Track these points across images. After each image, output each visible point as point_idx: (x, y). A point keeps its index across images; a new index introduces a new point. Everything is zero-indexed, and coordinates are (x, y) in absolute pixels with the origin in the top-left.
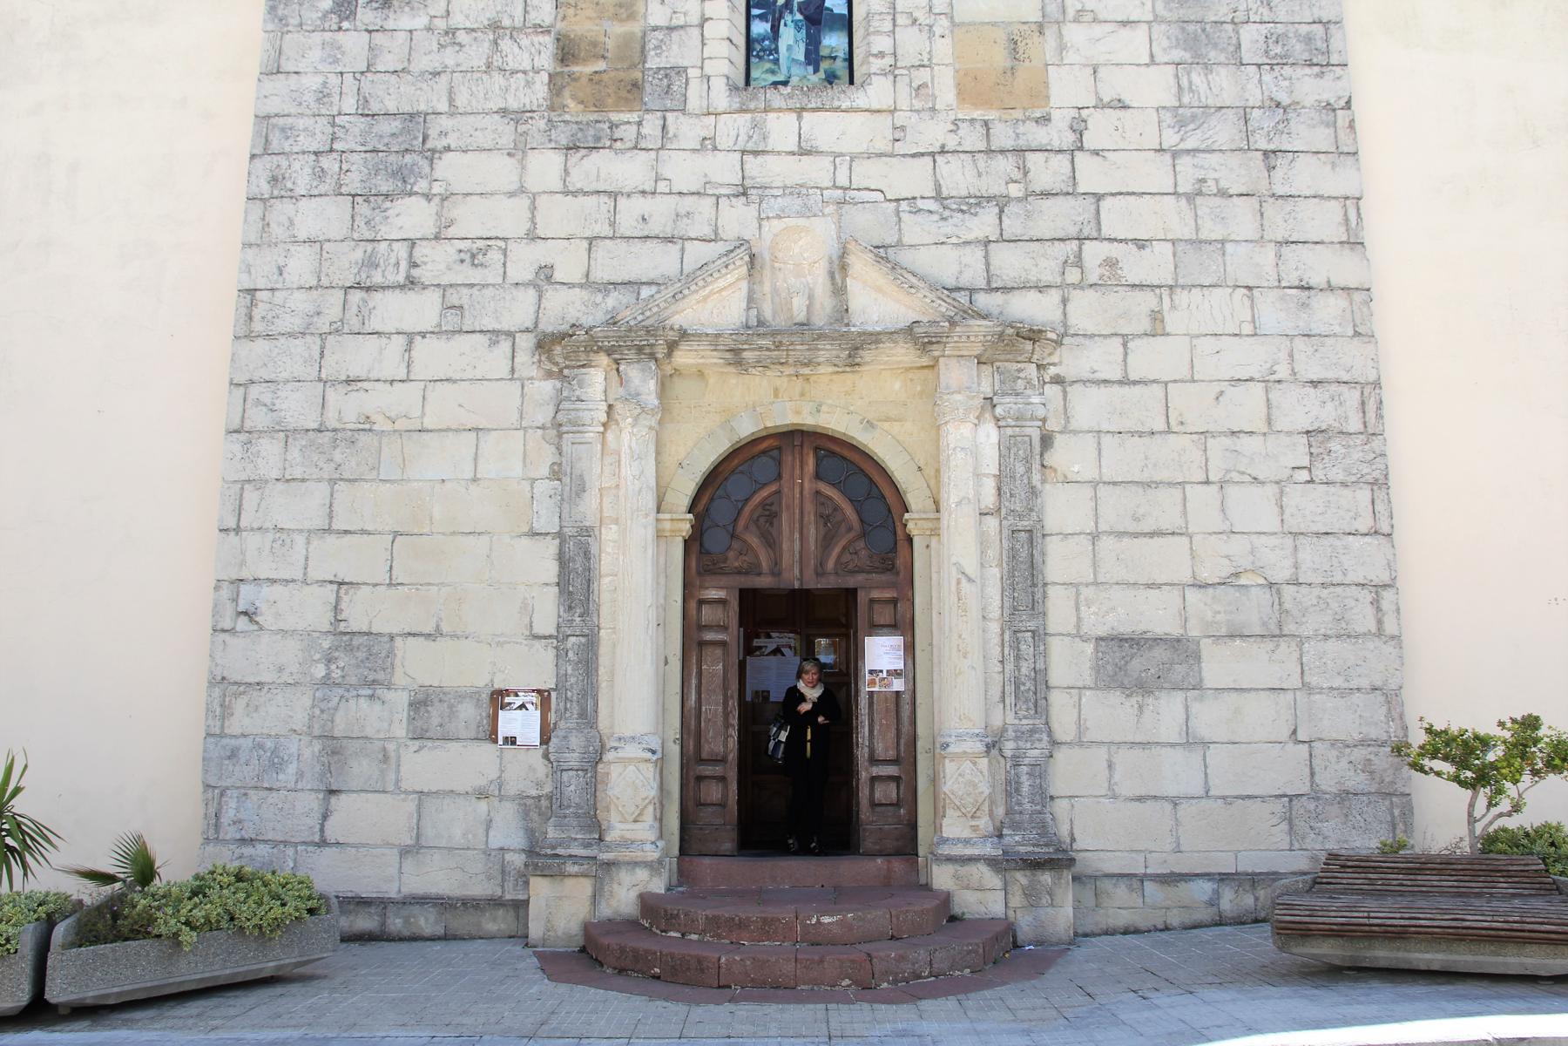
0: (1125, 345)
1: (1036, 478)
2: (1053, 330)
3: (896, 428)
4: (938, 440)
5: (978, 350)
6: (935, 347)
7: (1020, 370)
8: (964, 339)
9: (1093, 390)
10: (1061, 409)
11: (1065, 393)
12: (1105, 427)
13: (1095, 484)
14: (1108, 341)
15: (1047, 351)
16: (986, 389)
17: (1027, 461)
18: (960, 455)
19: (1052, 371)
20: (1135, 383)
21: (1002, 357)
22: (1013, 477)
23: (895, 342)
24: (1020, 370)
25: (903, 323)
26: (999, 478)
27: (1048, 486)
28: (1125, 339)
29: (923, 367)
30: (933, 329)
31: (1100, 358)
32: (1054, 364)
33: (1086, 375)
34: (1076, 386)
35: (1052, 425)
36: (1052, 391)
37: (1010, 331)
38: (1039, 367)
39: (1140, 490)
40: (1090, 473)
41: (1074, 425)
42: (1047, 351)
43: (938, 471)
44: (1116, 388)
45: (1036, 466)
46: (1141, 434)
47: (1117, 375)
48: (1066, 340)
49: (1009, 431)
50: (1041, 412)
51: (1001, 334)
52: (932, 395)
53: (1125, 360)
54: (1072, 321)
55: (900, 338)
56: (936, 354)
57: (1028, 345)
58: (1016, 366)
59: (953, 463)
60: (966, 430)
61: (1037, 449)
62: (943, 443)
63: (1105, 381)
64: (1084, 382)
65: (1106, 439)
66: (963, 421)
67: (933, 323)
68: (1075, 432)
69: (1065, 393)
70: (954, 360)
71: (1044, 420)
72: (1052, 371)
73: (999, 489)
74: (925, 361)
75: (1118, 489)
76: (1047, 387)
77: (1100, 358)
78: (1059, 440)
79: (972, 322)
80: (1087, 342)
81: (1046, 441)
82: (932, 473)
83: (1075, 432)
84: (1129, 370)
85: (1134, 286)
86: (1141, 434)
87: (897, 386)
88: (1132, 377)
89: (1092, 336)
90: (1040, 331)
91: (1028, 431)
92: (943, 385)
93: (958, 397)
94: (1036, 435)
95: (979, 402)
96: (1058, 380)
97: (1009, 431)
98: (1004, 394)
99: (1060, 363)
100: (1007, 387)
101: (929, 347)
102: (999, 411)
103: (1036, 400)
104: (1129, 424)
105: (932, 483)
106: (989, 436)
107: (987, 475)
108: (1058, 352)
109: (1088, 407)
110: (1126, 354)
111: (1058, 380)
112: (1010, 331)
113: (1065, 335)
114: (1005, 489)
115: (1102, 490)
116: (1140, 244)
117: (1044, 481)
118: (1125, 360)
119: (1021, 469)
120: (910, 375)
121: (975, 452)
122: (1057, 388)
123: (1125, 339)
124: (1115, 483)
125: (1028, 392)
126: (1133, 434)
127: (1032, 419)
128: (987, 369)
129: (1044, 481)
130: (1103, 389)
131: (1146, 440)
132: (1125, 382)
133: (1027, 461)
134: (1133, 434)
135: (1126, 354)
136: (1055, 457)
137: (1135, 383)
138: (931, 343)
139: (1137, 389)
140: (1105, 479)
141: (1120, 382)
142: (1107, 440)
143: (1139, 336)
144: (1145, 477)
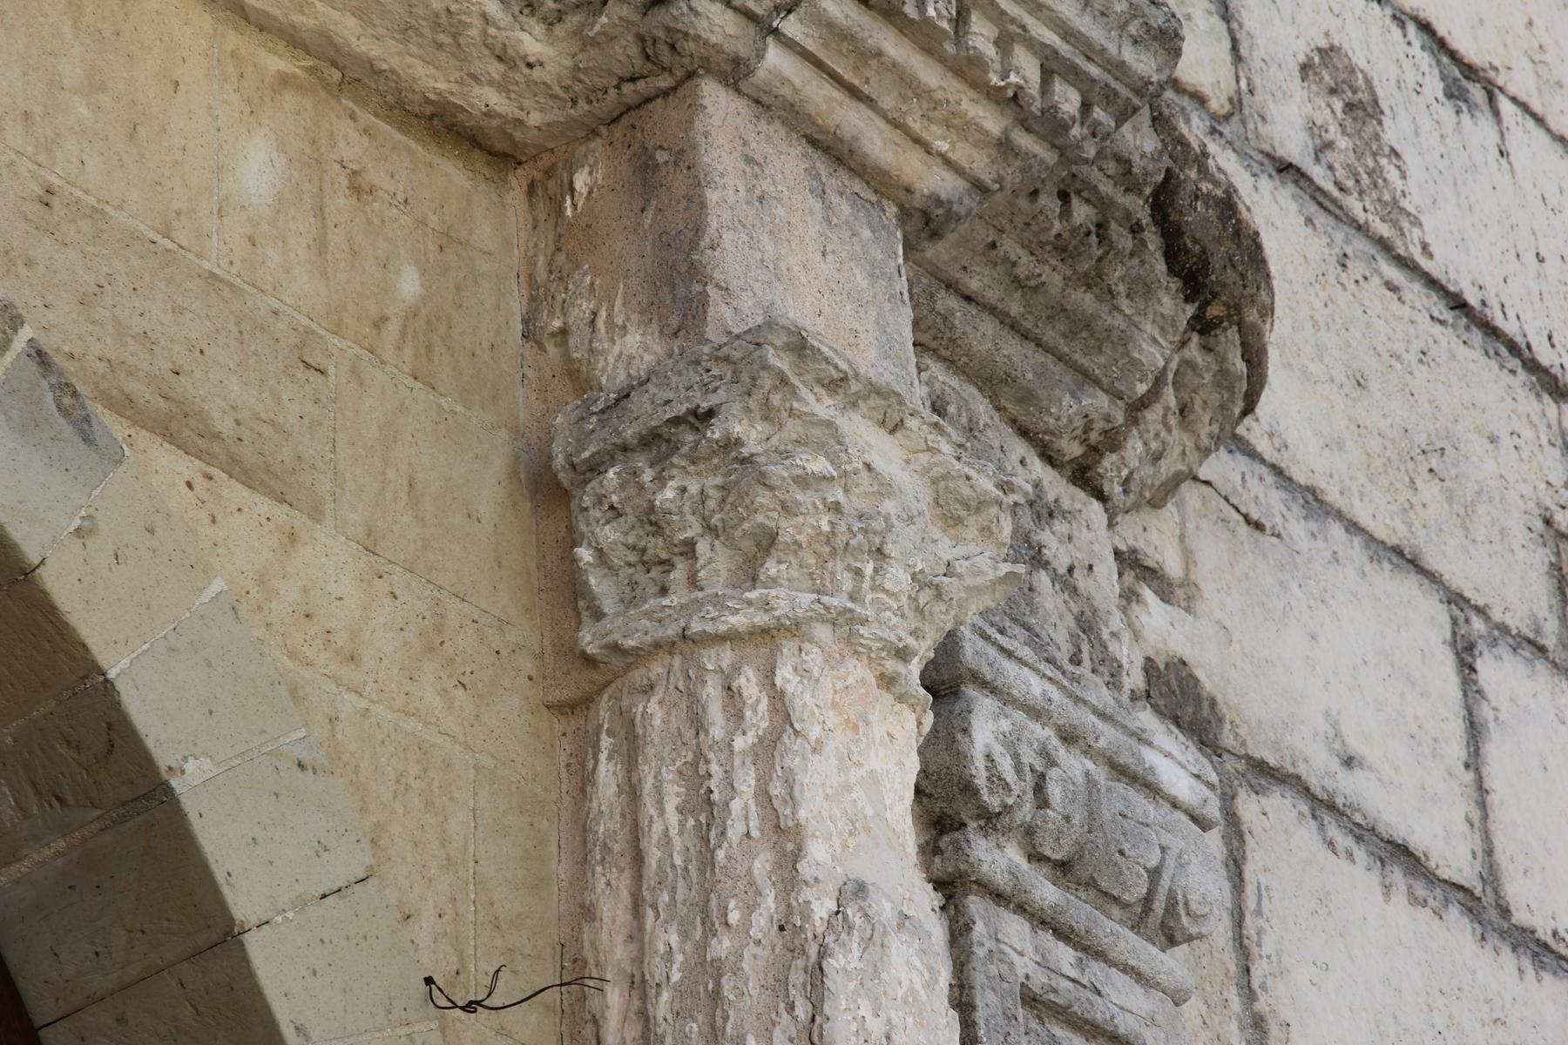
19: (1160, 627)
29: (447, 128)
57: (1155, 332)
72: (1160, 627)
80: (1298, 529)
85: (1458, 304)
87: (258, 170)
89: (1313, 502)
116: (1467, 81)
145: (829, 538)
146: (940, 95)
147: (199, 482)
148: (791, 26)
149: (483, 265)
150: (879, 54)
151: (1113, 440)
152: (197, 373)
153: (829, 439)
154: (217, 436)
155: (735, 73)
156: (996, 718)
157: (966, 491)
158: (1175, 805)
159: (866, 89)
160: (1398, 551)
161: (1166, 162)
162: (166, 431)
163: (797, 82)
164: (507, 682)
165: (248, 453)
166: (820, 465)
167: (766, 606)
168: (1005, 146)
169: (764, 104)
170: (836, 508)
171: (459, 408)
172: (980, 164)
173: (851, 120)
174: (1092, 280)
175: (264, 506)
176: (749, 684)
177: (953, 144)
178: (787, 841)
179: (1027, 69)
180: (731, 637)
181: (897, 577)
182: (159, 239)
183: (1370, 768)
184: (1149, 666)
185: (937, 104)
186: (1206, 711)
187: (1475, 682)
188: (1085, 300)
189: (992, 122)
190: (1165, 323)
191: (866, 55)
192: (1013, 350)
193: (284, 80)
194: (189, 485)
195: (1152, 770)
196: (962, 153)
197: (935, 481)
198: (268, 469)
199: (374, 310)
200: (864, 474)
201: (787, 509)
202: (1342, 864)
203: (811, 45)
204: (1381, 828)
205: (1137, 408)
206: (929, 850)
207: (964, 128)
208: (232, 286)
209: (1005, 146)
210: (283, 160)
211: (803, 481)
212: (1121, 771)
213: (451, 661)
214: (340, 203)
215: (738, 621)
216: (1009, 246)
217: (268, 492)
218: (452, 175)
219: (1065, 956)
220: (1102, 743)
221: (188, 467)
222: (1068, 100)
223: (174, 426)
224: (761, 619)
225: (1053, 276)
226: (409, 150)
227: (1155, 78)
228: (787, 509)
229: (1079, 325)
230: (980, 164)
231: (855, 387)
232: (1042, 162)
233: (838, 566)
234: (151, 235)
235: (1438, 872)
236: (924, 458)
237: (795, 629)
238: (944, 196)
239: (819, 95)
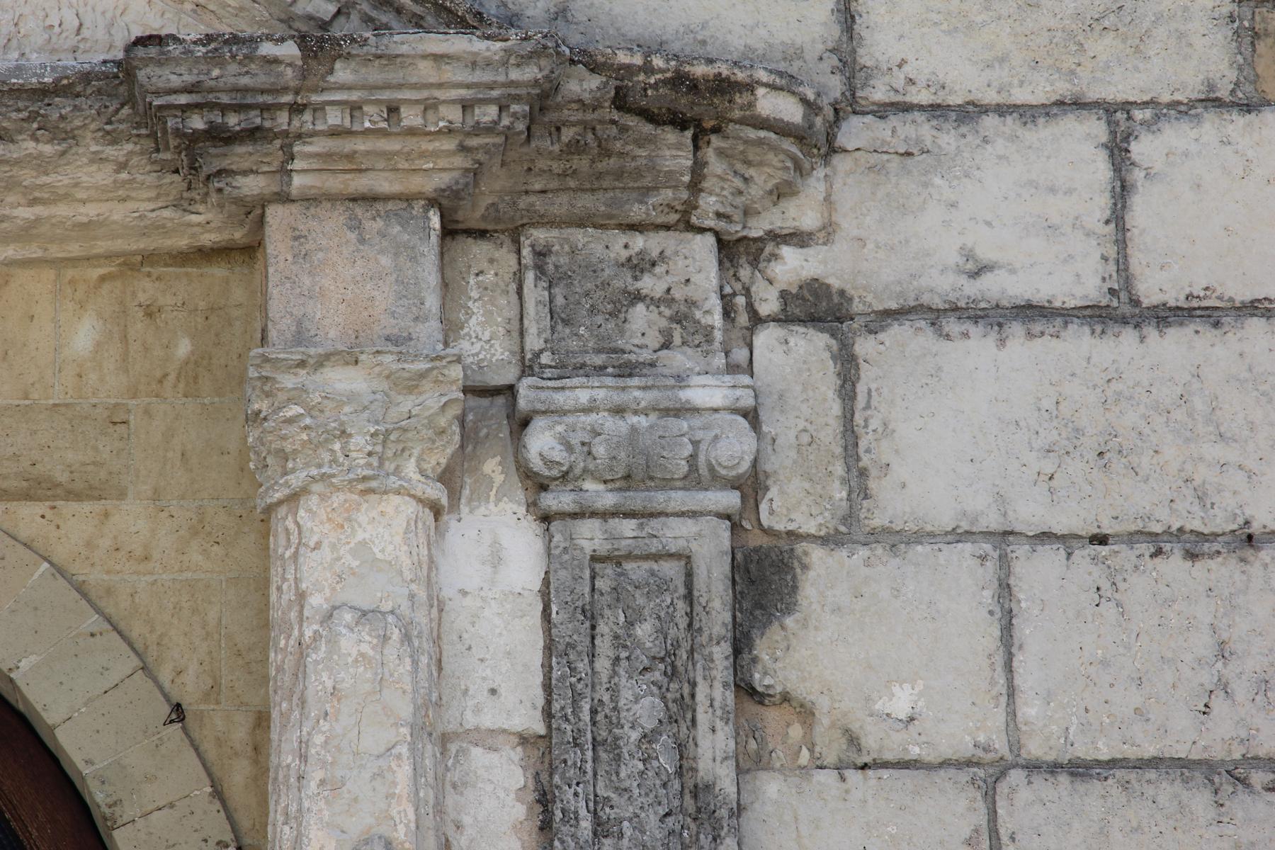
0: (1118, 151)
1: (714, 747)
2: (787, 83)
3: (72, 529)
4: (263, 584)
5: (439, 169)
6: (240, 155)
7: (640, 265)
8: (372, 117)
9: (975, 351)
10: (830, 433)
11: (848, 366)
12: (1031, 512)
13: (988, 773)
14: (1043, 132)
15: (763, 180)
16: (486, 343)
17: (673, 668)
18: (354, 643)
19: (792, 266)
20: (1165, 316)
21: (560, 205)
22: (607, 746)
23: (65, 136)
24: (640, 265)
25: (102, 48)
26: (543, 749)
27: (771, 787)
28: (1121, 126)
30: (229, 74)
31: (1013, 212)
32: (799, 238)
33: (943, 284)
34: (896, 332)
35: (791, 507)
36: (792, 356)
37: (583, 85)
38: (731, 250)
39: (1200, 801)
40: (966, 725)
41: (891, 504)
42: (763, 180)
43: (262, 721)
44: (1079, 344)
45: (713, 691)
46: (1195, 546)
47: (1082, 281)
48: (854, 132)
49: (590, 536)
50: (733, 448)
51: (543, 100)
52: (231, 372)
53: (1118, 217)
54: (883, 42)
55: (82, 115)
56: (251, 186)
57: (673, 151)
58: (620, 245)
59: (319, 681)
60: (387, 526)
61: (718, 612)
62: (281, 598)
63: (1032, 313)
64: (935, 315)
65: (1038, 572)
66: (367, 487)
67: (223, 45)
68: (896, 539)
69: (848, 366)
70: (329, 228)
71: (752, 485)
72: (792, 266)
73: (544, 799)
74: (206, 224)
75: (1094, 799)
76: (766, 338)
77: (1013, 212)
78: (824, 577)
79: (406, 42)
80: (948, 139)
81: (764, 580)
82: (240, 734)
83: (896, 539)
84: (1137, 260)
86: (1195, 546)
87: (84, 335)
88: (1155, 287)
89: (968, 113)
90: (724, 86)
91: (676, 533)
92: (281, 327)
93: (341, 379)
94: (710, 548)
95: (436, 401)
96: (817, 308)
97: (590, 536)
98: (567, 369)
99: (828, 231)
100: (579, 340)
101: (214, 160)
102: (542, 442)
103: (709, 392)
104: (1144, 500)
105: (238, 776)
106: (499, 558)
107: (487, 738)
108: (815, 186)
109: (957, 424)
110: (1122, 191)
111: (817, 308)
112: (583, 85)
113: (848, 106)
114: (572, 799)
115: (1024, 802)
117: (749, 763)
118: (1118, 217)
119: (642, 707)
120: (146, 289)
121: (429, 638)
122: (811, 346)
123: (1121, 126)
124: (1080, 770)
125: (679, 359)
126: (1157, 543)
127: (695, 478)
128: (488, 263)
129: (749, 763)
130: (1023, 352)
131: (1221, 570)
132: (1120, 310)
133: (673, 668)
134: (1157, 543)
135: (1122, 191)
136: (802, 655)
137: (1165, 316)
138: (219, 136)
139: (1174, 348)
140: (1035, 748)
141: (1099, 316)
142: (1038, 572)
143: (1183, 110)
144: (1218, 737)
145: (310, 441)
146: (406, 150)
147: (49, 514)
148: (298, 164)
149: (236, 313)
150: (355, 152)
151: (690, 206)
152: (46, 459)
153: (299, 394)
154: (59, 485)
155: (284, 198)
156: (551, 428)
157: (406, 375)
158: (716, 410)
159: (363, 167)
160: (1060, 103)
161: (613, 83)
162: (27, 496)
163: (318, 184)
164: (246, 529)
165: (79, 486)
166: (295, 410)
167: (287, 484)
168: (463, 148)
169: (311, 200)
170: (306, 428)
171: (216, 399)
172: (460, 161)
173: (361, 184)
174: (606, 153)
175: (87, 507)
176: (290, 523)
177: (434, 163)
178: (302, 596)
179: (455, 114)
180: (280, 503)
181: (359, 441)
182: (22, 402)
183: (1000, 267)
184: (784, 295)
185: (409, 154)
186: (836, 299)
187: (1129, 159)
188: (613, 162)
189: (449, 144)
190: (679, 146)
191: (350, 157)
192: (586, 202)
193: (103, 279)
194: (43, 517)
195: (688, 401)
196: (442, 163)
197: (388, 377)
198: (91, 488)
199: (158, 374)
200: (326, 401)
201: (284, 438)
202: (960, 345)
203: (315, 166)
204: (1005, 303)
205: (695, 186)
206: (532, 505)
207: (435, 154)
208: (67, 405)
209: (463, 148)
210: (101, 322)
211: (290, 421)
212: (667, 412)
213: (210, 533)
214: (138, 327)
215: (278, 496)
216: (541, 164)
217: (90, 498)
218: (218, 271)
219: (628, 527)
220: (643, 404)
221: (40, 508)
222: (488, 114)
223: (32, 492)
224: (287, 491)
225: (581, 163)
226: (187, 274)
227: (539, 76)
228: (284, 438)
229: (619, 174)
230: (460, 161)
231: (311, 361)
232: (494, 145)
233: (320, 450)
234: (17, 402)
235: (1066, 306)
236: (377, 369)
237: (304, 491)
238: (443, 186)
239: (334, 183)
